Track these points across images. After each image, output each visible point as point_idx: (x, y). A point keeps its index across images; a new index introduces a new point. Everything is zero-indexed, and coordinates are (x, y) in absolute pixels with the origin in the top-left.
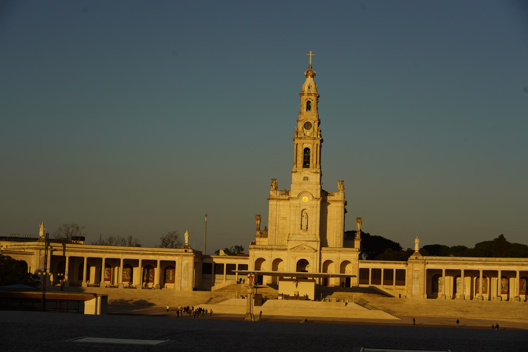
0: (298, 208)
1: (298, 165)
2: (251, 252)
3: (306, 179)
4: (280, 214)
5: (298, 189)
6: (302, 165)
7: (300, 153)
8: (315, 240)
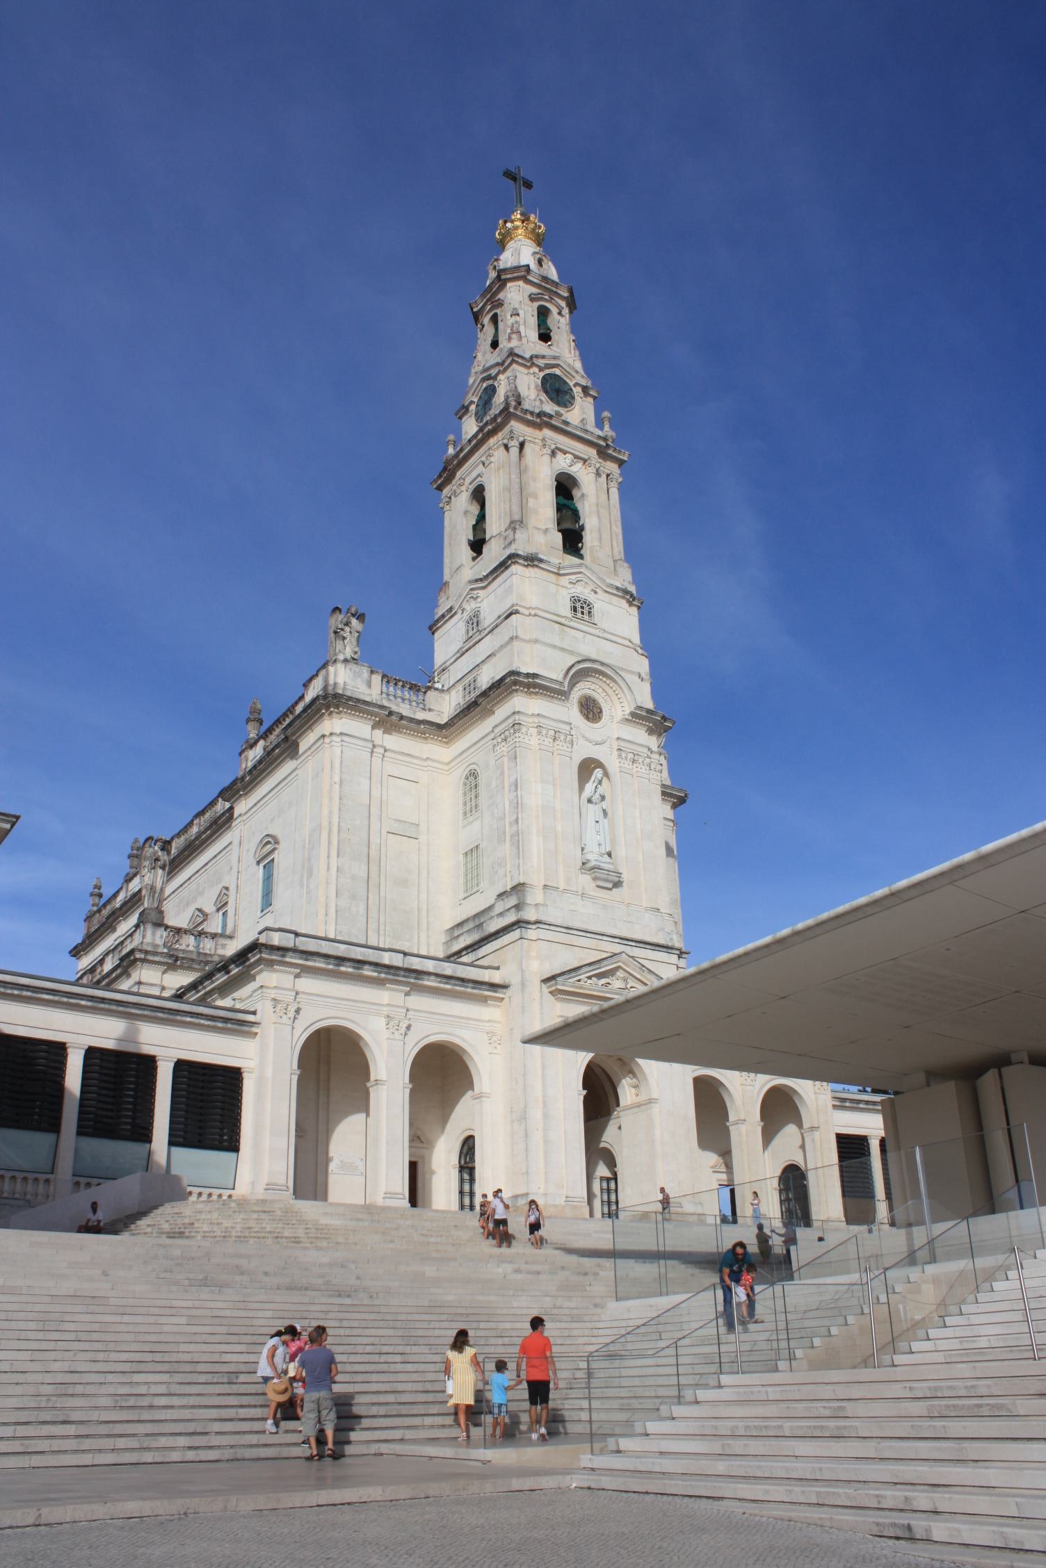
0: (561, 746)
4: (384, 798)
5: (554, 647)
8: (662, 942)
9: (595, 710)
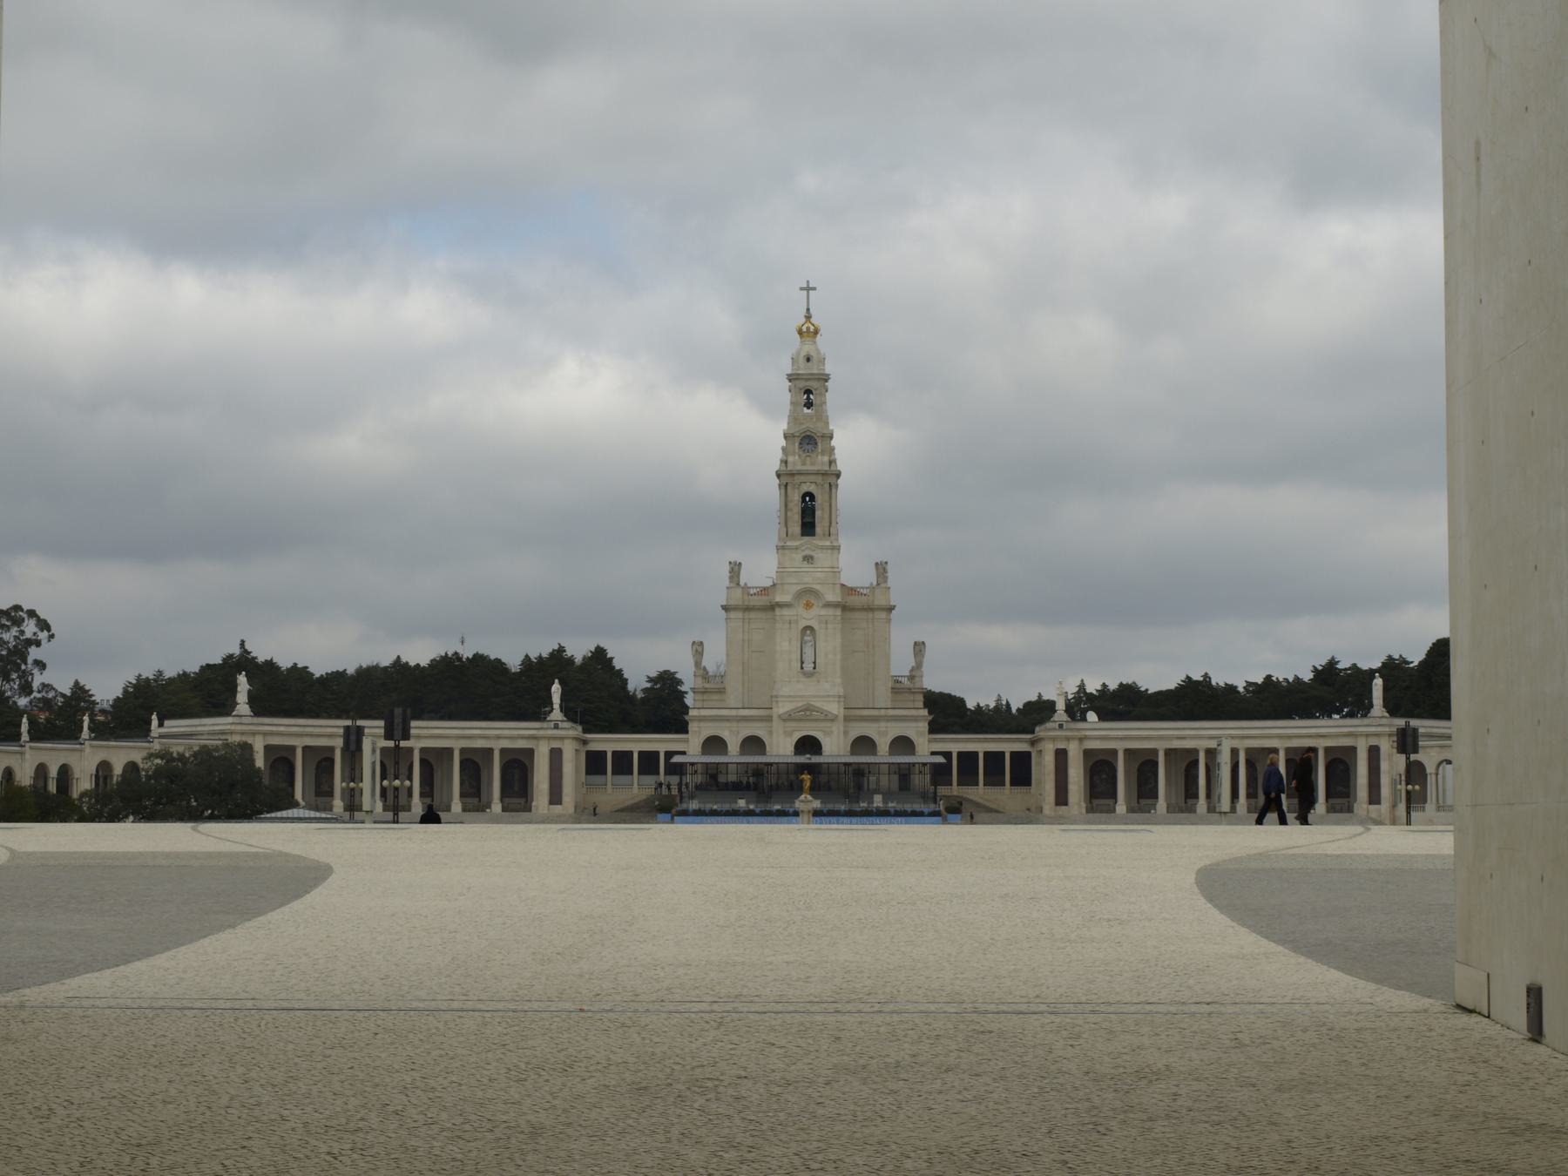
2: (692, 727)
3: (808, 559)
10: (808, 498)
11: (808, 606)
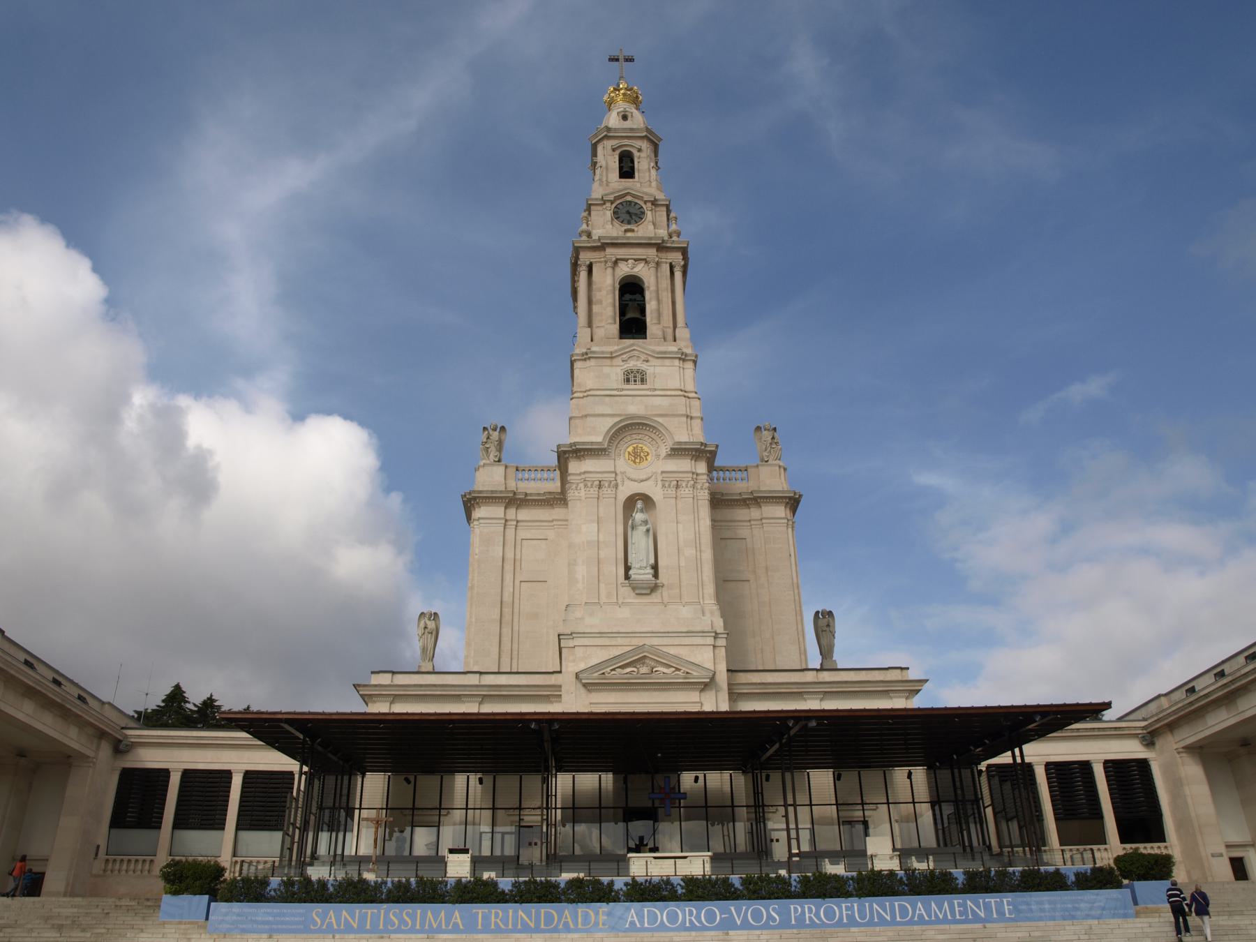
0: (607, 491)
1: (599, 333)
3: (634, 377)
4: (518, 557)
5: (603, 415)
6: (615, 328)
7: (604, 292)
9: (642, 454)
10: (631, 290)
11: (637, 456)
